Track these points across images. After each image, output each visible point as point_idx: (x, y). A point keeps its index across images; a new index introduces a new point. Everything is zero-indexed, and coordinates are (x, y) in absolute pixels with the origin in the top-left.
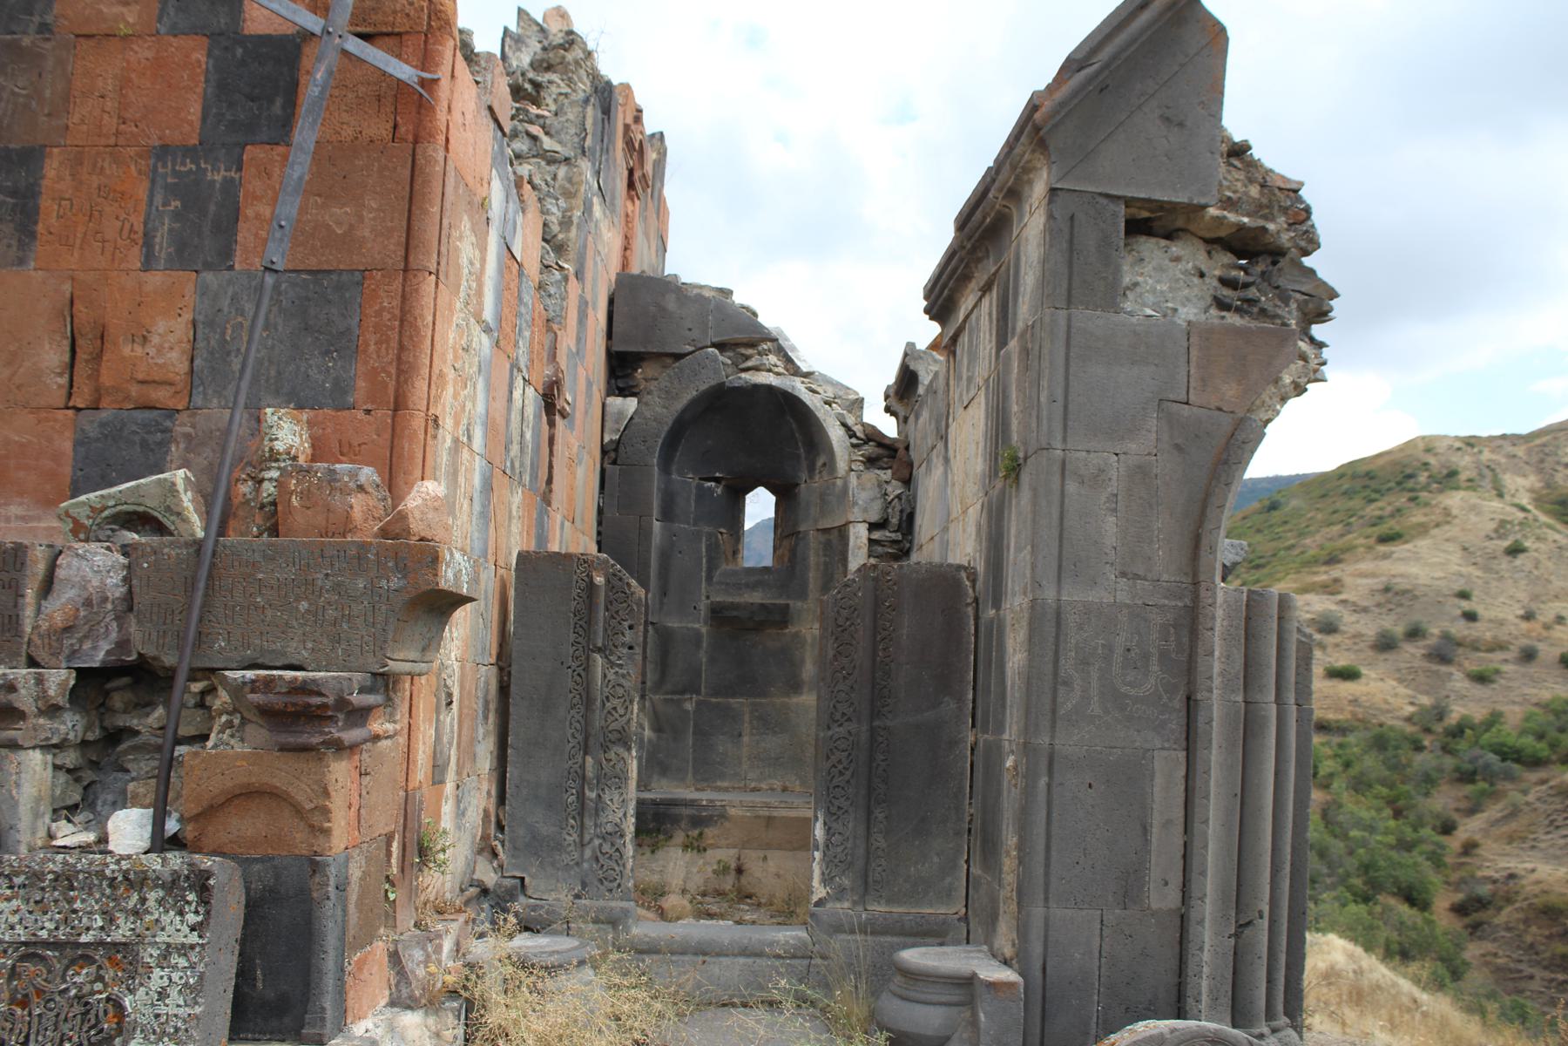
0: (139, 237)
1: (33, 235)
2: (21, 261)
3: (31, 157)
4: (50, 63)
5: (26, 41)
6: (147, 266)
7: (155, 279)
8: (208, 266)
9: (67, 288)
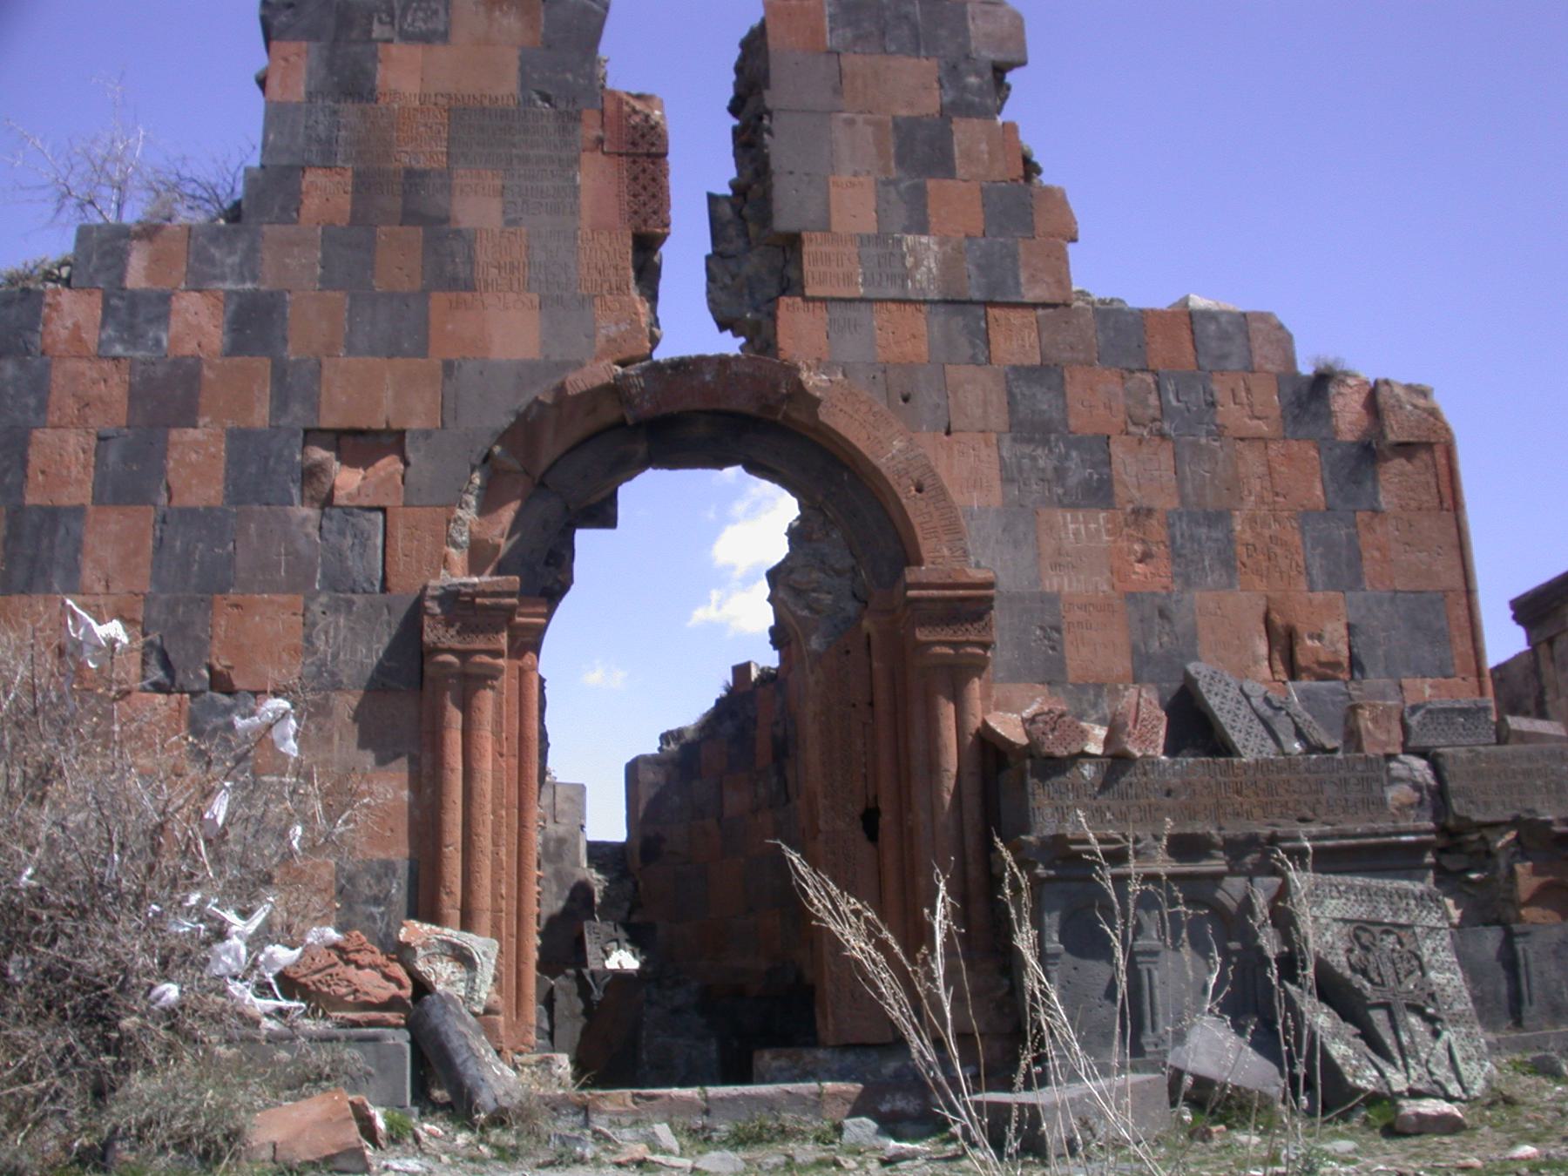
0: (1302, 569)
1: (1235, 568)
2: (1231, 585)
3: (1219, 518)
4: (1221, 455)
5: (1203, 441)
6: (1311, 590)
7: (1319, 597)
8: (1350, 589)
9: (1262, 603)
